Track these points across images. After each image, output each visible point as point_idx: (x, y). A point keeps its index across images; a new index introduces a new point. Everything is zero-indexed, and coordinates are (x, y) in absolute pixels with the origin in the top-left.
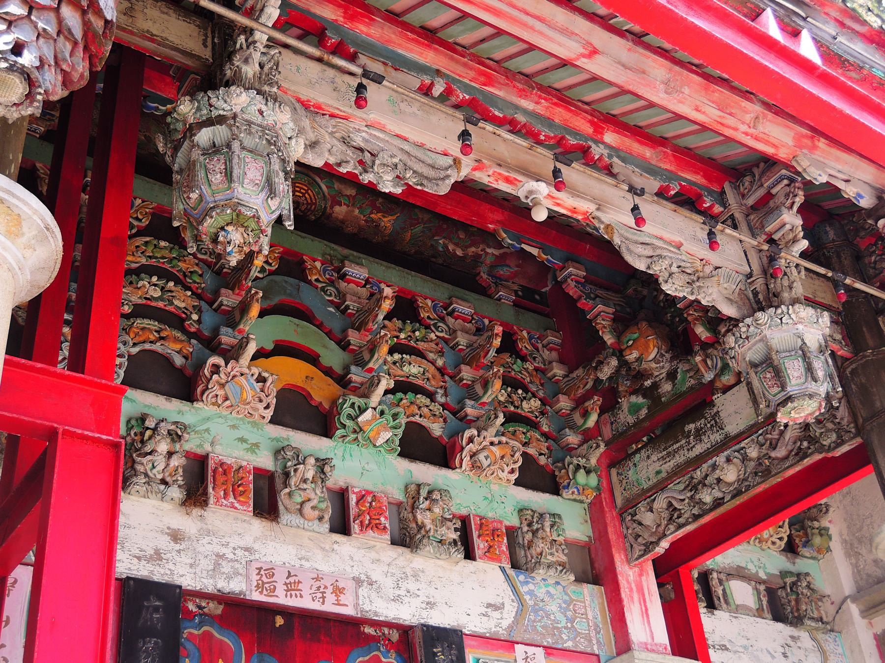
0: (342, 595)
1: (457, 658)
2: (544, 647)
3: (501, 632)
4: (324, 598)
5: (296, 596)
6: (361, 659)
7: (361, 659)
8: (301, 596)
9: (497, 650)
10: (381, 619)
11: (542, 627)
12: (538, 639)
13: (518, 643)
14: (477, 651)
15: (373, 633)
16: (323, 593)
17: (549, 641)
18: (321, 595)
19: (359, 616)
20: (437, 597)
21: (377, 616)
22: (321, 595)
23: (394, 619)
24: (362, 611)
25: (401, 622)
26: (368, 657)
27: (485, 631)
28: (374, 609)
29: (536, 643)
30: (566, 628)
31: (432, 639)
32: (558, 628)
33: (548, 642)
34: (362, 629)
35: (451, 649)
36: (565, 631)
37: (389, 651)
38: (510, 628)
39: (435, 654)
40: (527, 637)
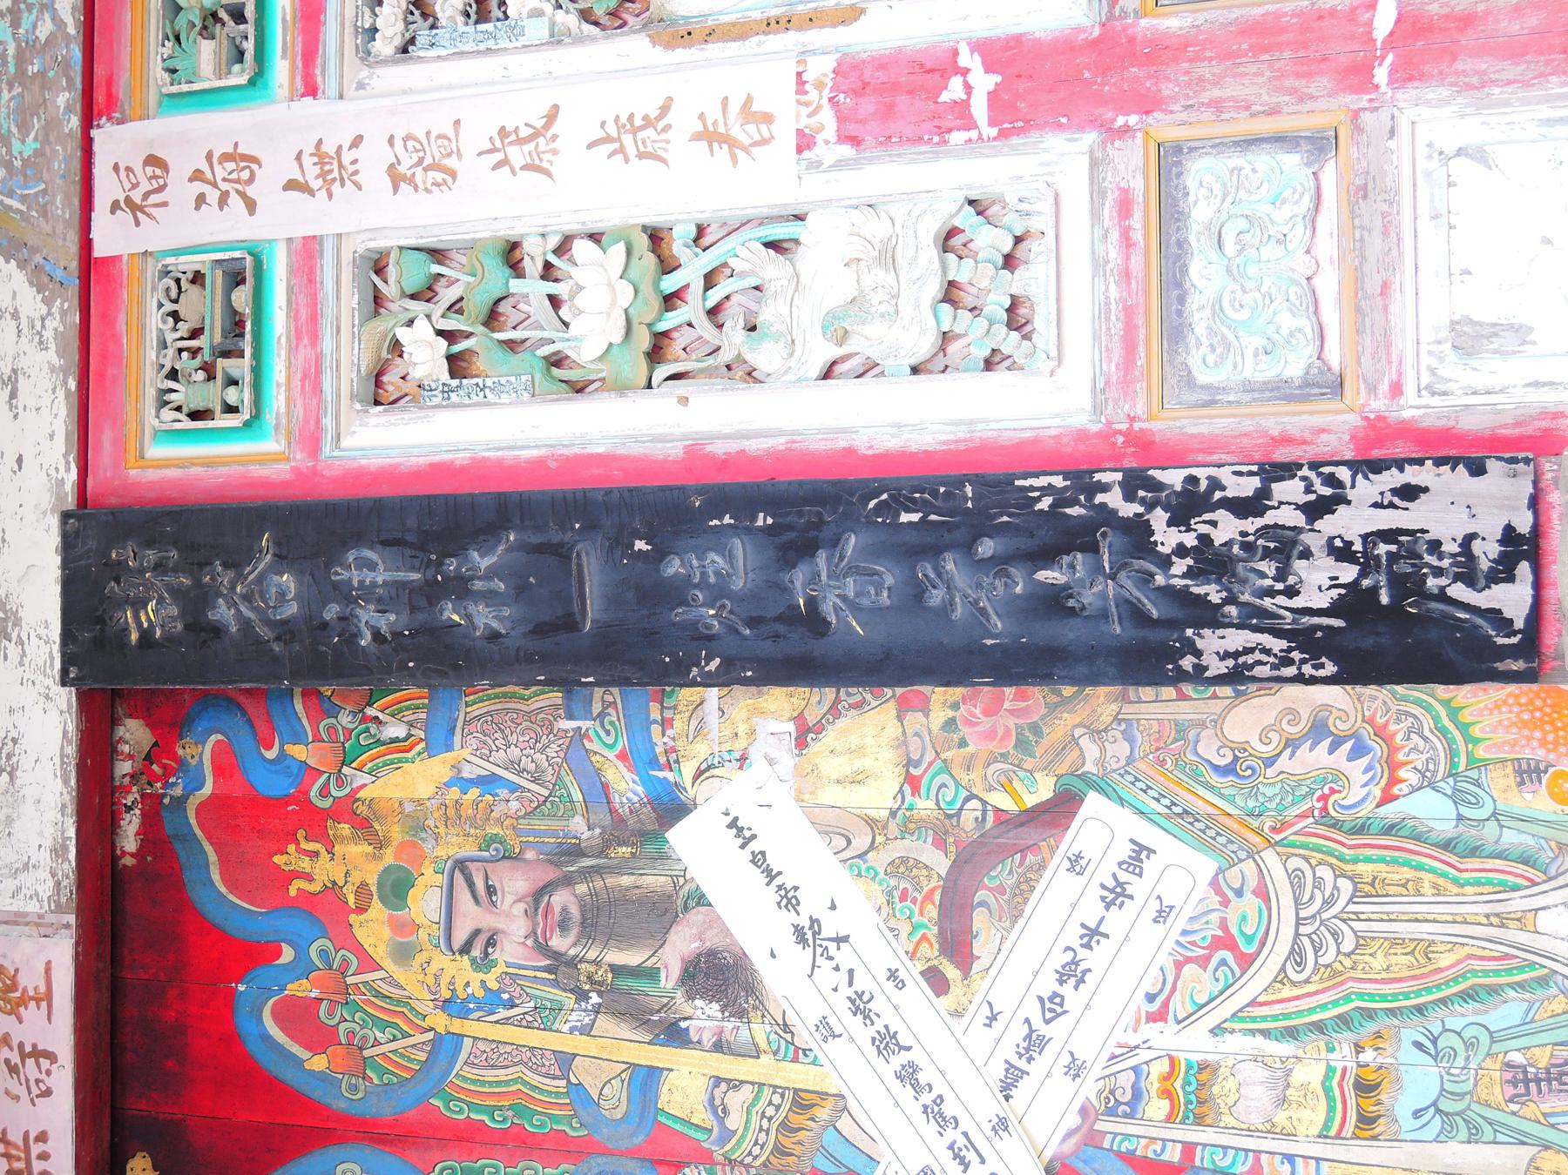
0: (24, 980)
1: (149, 544)
2: (88, 122)
3: (53, 323)
4: (38, 1054)
5: (44, 1156)
6: (216, 876)
7: (216, 876)
8: (42, 1137)
9: (116, 338)
10: (71, 832)
11: (24, 128)
12: (65, 156)
13: (86, 244)
14: (132, 427)
15: (136, 821)
16: (24, 1056)
17: (65, 99)
18: (30, 1062)
19: (71, 919)
21: (65, 848)
22: (30, 1062)
23: (66, 782)
24: (59, 909)
25: (71, 750)
26: (208, 848)
27: (61, 394)
28: (44, 857)
29: (76, 164)
30: (15, 24)
31: (99, 643)
32: (21, 59)
33: (69, 109)
34: (128, 861)
35: (121, 564)
36: (27, 21)
37: (179, 761)
38: (40, 279)
39: (146, 635)
40: (64, 208)
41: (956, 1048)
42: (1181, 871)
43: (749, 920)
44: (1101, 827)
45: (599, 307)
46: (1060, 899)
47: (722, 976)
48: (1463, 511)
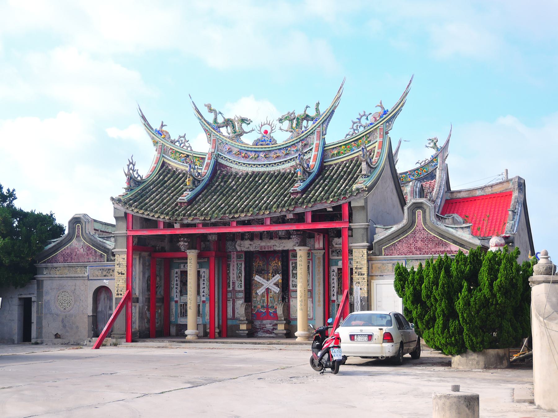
20: (285, 245)
41: (272, 284)
42: (277, 292)
43: (275, 277)
44: (279, 289)
45: (294, 272)
46: (276, 288)
47: (274, 276)
48: (287, 300)
